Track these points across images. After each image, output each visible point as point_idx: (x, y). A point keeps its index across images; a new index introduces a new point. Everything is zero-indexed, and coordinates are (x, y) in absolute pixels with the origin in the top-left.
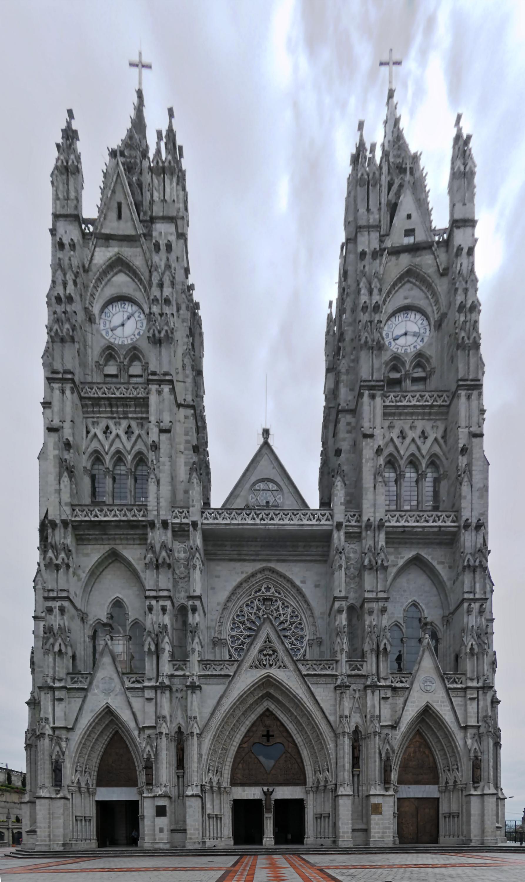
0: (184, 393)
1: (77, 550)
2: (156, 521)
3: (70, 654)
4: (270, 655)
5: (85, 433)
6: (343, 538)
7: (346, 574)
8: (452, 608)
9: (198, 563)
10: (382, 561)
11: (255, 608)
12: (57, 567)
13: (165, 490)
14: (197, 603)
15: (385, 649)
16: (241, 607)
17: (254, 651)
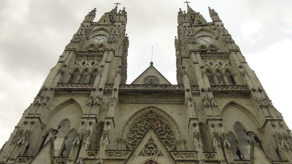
0: (119, 53)
1: (53, 99)
2: (96, 89)
3: (26, 145)
4: (153, 148)
5: (74, 63)
6: (191, 95)
7: (195, 109)
8: (262, 125)
9: (115, 104)
10: (214, 103)
11: (144, 124)
12: (40, 105)
13: (104, 79)
14: (111, 121)
15: (227, 145)
16: (136, 124)
17: (141, 147)
